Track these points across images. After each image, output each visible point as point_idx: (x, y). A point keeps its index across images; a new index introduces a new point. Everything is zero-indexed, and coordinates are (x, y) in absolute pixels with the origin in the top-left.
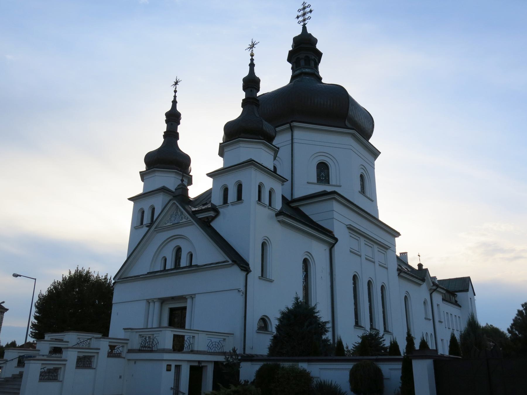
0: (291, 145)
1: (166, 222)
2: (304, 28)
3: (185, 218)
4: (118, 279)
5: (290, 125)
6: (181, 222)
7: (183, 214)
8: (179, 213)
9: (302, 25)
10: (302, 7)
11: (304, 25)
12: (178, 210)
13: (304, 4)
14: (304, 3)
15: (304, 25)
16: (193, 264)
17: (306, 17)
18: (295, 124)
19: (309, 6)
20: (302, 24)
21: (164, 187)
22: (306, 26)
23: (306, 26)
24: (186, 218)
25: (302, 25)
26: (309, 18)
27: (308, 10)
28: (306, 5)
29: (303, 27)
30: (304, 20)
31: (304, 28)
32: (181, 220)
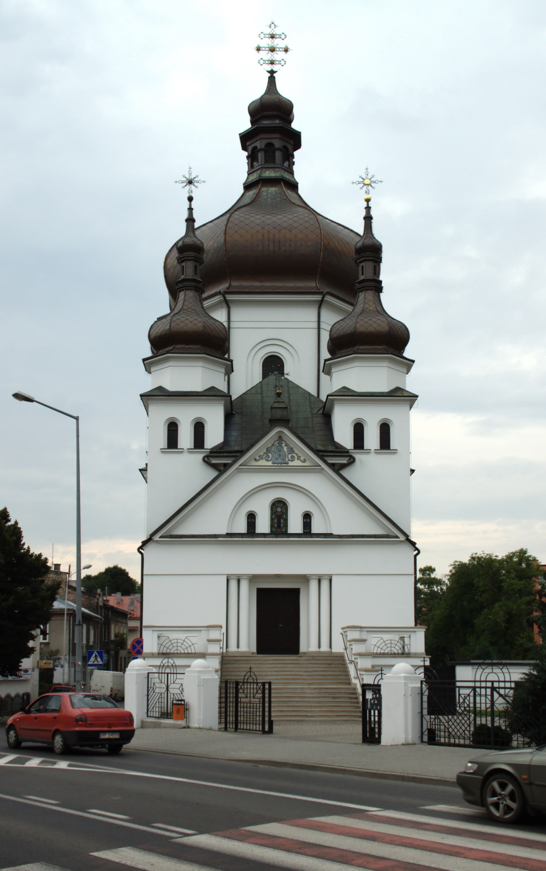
0: (316, 330)
1: (258, 458)
2: (272, 80)
3: (299, 458)
4: (161, 537)
5: (323, 298)
6: (291, 463)
7: (294, 451)
8: (285, 449)
9: (268, 72)
10: (268, 31)
11: (272, 72)
12: (282, 443)
13: (273, 26)
14: (272, 24)
15: (272, 72)
16: (315, 529)
17: (278, 56)
18: (328, 298)
19: (283, 36)
20: (269, 68)
21: (213, 388)
22: (275, 75)
23: (275, 75)
24: (302, 458)
25: (268, 72)
26: (282, 63)
27: (278, 43)
28: (277, 31)
29: (269, 78)
30: (272, 63)
31: (272, 80)
32: (292, 461)
